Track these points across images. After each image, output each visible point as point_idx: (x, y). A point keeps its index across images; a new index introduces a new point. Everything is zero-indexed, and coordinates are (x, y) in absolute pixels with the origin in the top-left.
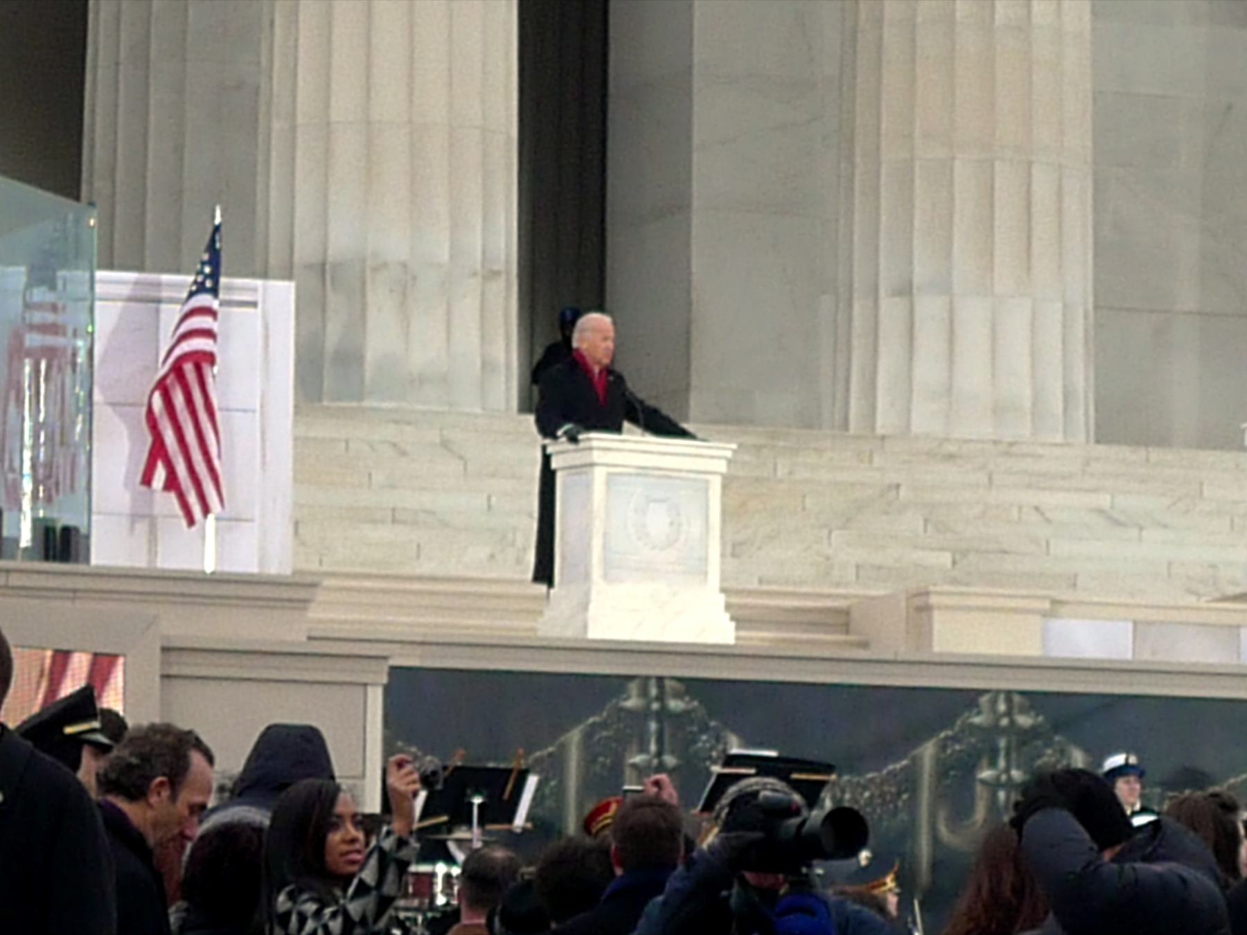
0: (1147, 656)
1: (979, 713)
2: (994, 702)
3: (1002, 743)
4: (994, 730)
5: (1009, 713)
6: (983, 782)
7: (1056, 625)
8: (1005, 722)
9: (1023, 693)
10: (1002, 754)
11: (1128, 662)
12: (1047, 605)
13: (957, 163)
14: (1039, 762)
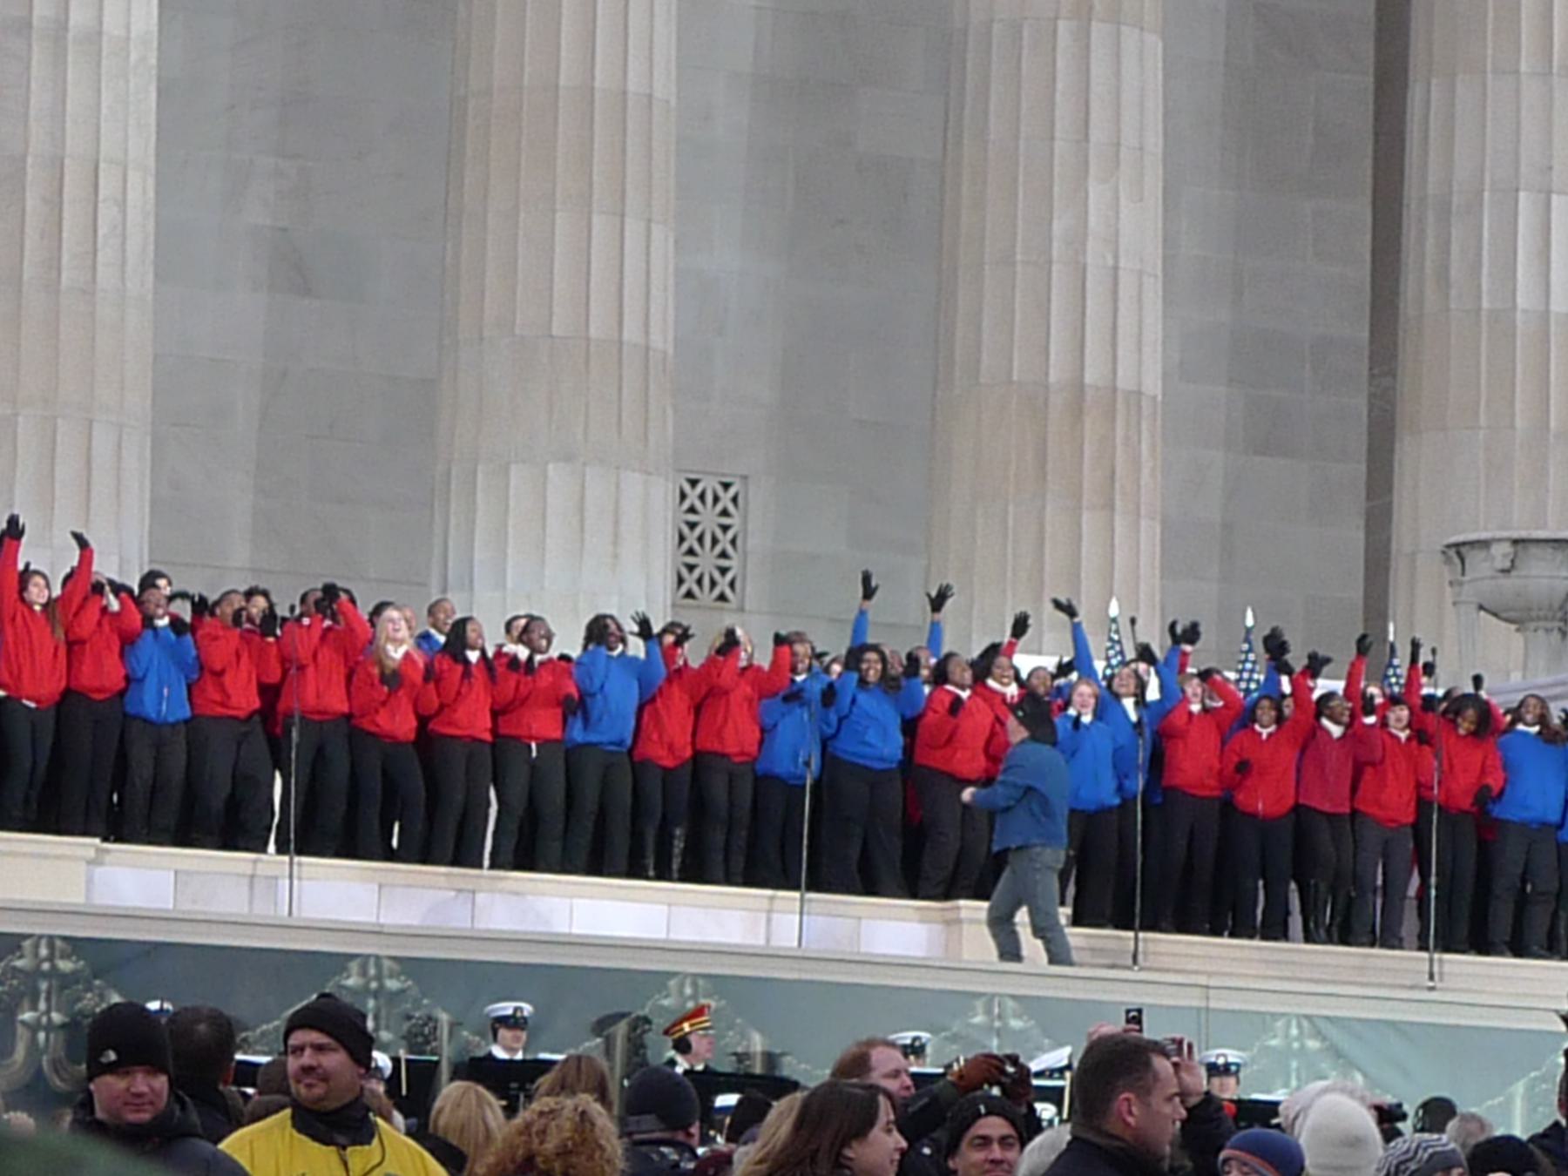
0: (187, 907)
1: (21, 957)
2: (37, 946)
3: (44, 986)
4: (37, 973)
5: (51, 958)
6: (23, 1023)
7: (98, 870)
8: (46, 966)
9: (65, 939)
10: (43, 996)
11: (167, 911)
12: (92, 853)
13: (20, 419)
14: (79, 1006)
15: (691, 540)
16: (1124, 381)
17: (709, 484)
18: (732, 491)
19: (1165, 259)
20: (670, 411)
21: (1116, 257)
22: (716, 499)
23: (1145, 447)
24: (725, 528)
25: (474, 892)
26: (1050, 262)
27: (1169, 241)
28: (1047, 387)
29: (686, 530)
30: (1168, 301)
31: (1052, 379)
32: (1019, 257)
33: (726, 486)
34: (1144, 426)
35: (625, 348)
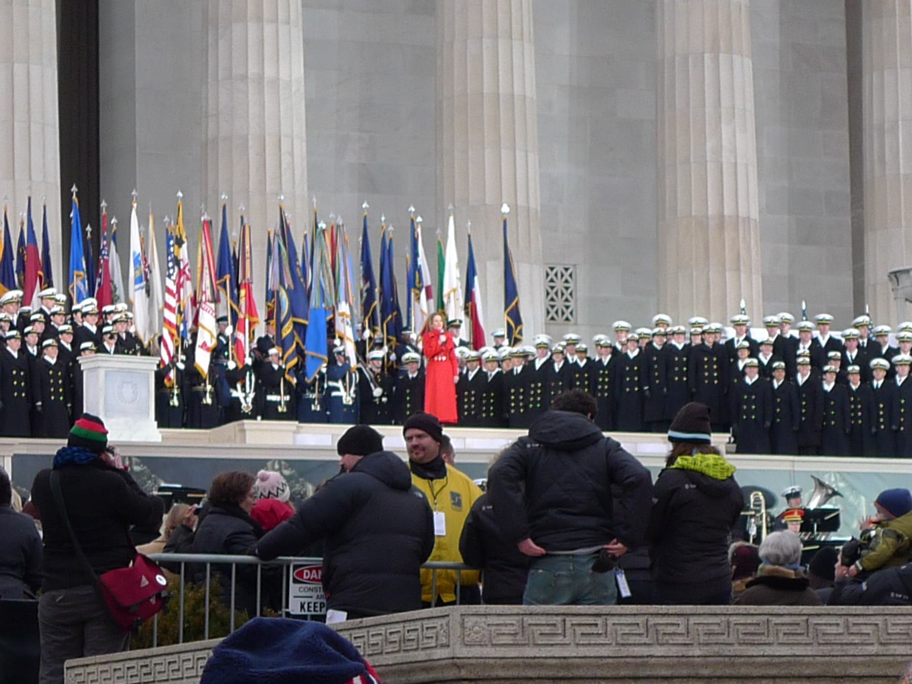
15: (552, 294)
16: (742, 213)
17: (559, 269)
18: (569, 272)
19: (758, 159)
20: (540, 237)
21: (736, 158)
22: (562, 276)
23: (752, 241)
24: (567, 288)
25: (465, 438)
26: (706, 162)
27: (759, 151)
28: (707, 218)
29: (550, 290)
30: (760, 177)
31: (710, 213)
32: (692, 160)
33: (566, 269)
34: (752, 233)
35: (519, 210)
